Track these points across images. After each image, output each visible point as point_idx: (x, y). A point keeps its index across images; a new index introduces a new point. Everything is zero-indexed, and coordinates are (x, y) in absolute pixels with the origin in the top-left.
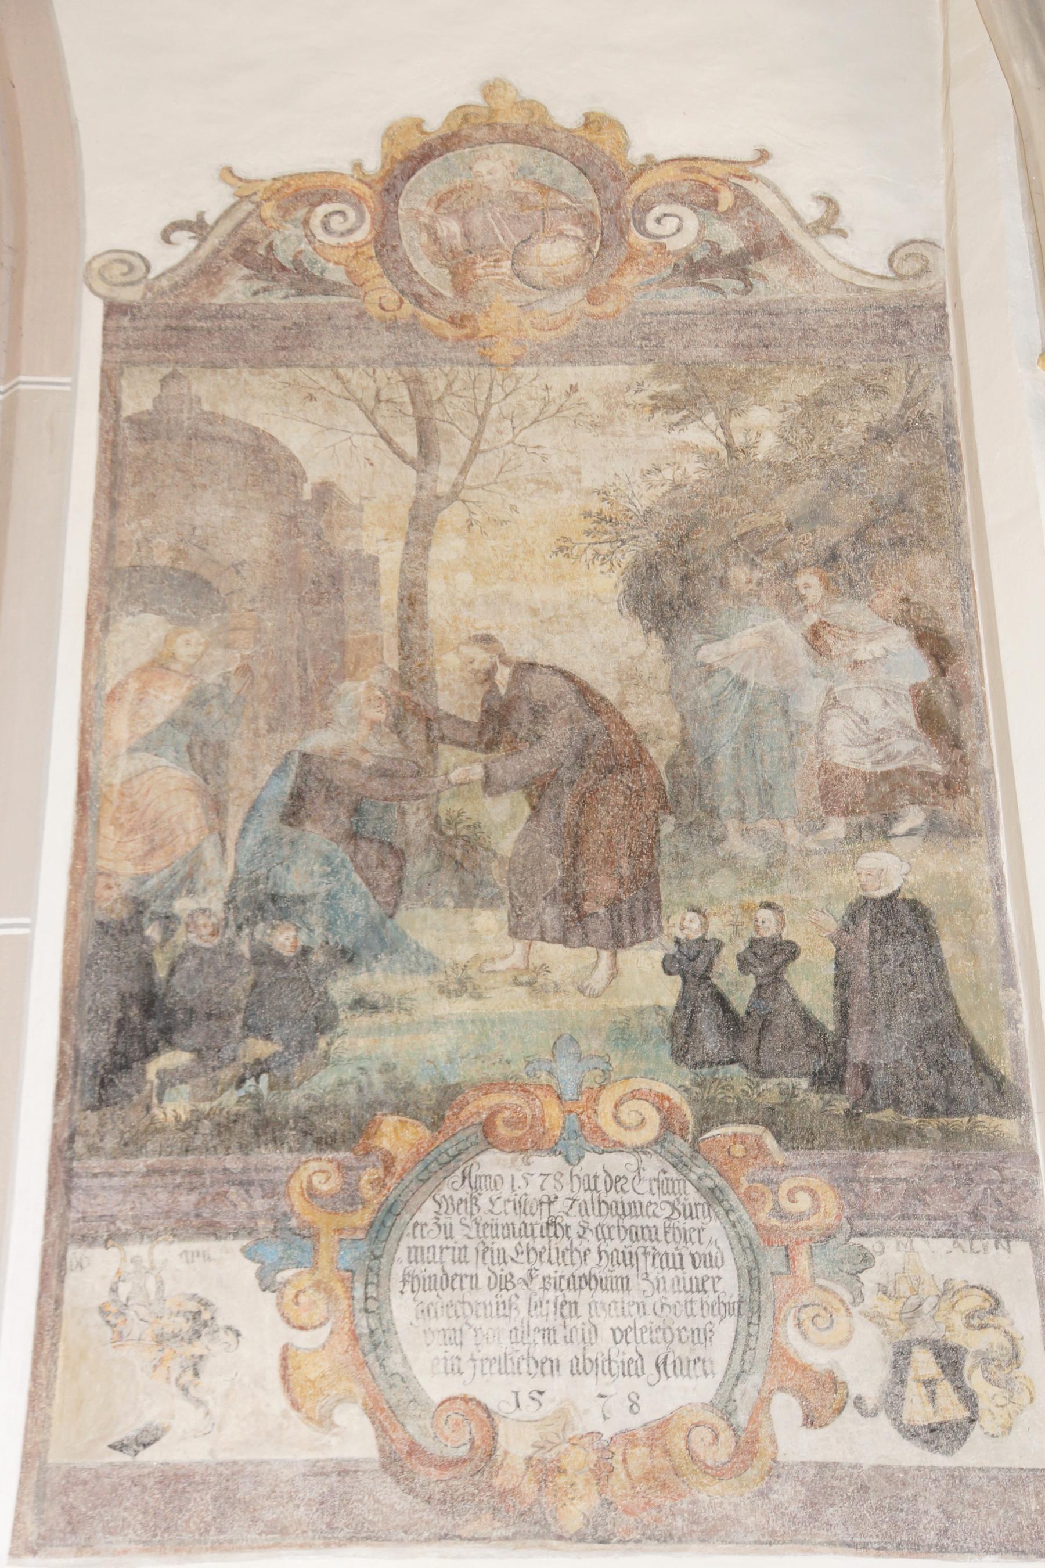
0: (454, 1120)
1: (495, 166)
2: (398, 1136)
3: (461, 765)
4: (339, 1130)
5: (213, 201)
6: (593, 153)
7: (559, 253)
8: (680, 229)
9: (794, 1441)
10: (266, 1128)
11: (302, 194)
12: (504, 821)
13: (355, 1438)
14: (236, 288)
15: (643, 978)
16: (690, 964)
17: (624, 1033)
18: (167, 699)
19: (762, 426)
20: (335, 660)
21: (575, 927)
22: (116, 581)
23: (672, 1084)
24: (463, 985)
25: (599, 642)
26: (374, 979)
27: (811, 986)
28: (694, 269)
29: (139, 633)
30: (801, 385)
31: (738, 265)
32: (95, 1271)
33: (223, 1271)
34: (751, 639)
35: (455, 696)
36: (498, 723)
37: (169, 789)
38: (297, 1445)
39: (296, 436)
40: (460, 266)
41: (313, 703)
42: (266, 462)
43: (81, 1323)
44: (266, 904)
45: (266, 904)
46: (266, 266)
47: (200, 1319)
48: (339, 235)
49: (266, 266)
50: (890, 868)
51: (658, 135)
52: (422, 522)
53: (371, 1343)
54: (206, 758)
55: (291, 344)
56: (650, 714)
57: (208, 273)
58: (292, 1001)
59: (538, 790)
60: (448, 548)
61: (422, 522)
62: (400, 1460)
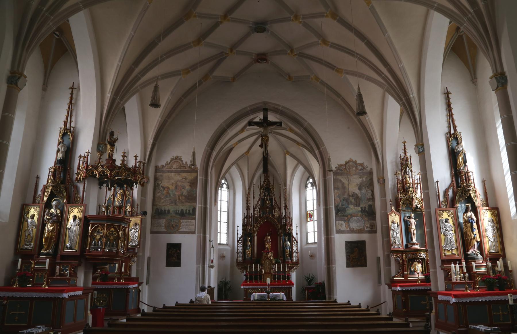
0: (352, 215)
1: (351, 163)
2: (349, 216)
3: (351, 198)
4: (347, 216)
5: (337, 166)
6: (355, 162)
7: (354, 169)
8: (360, 167)
9: (366, 229)
10: (344, 216)
11: (341, 165)
12: (353, 201)
13: (348, 229)
14: (339, 171)
15: (360, 209)
16: (361, 208)
17: (359, 211)
18: (337, 195)
19: (364, 179)
20: (345, 192)
21: (356, 206)
22: (334, 188)
23: (361, 214)
24: (352, 209)
25: (357, 191)
26: (348, 209)
27: (367, 209)
28: (361, 170)
29: (336, 191)
30: (366, 177)
31: (363, 170)
32: (337, 222)
33: (343, 222)
34: (364, 191)
35: (350, 194)
36: (353, 196)
37: (338, 199)
38: (346, 230)
39: (342, 180)
40: (349, 169)
41: (344, 195)
42: (341, 181)
43: (337, 224)
44: (343, 205)
45: (343, 205)
46: (340, 170)
47: (342, 224)
48: (344, 167)
49: (340, 170)
50: (370, 203)
51: (358, 162)
52: (348, 185)
53: (349, 225)
54: (340, 197)
55: (341, 174)
56: (359, 195)
57: (337, 170)
58: (344, 210)
59: (354, 199)
60: (350, 186)
61: (348, 185)
62: (350, 230)
